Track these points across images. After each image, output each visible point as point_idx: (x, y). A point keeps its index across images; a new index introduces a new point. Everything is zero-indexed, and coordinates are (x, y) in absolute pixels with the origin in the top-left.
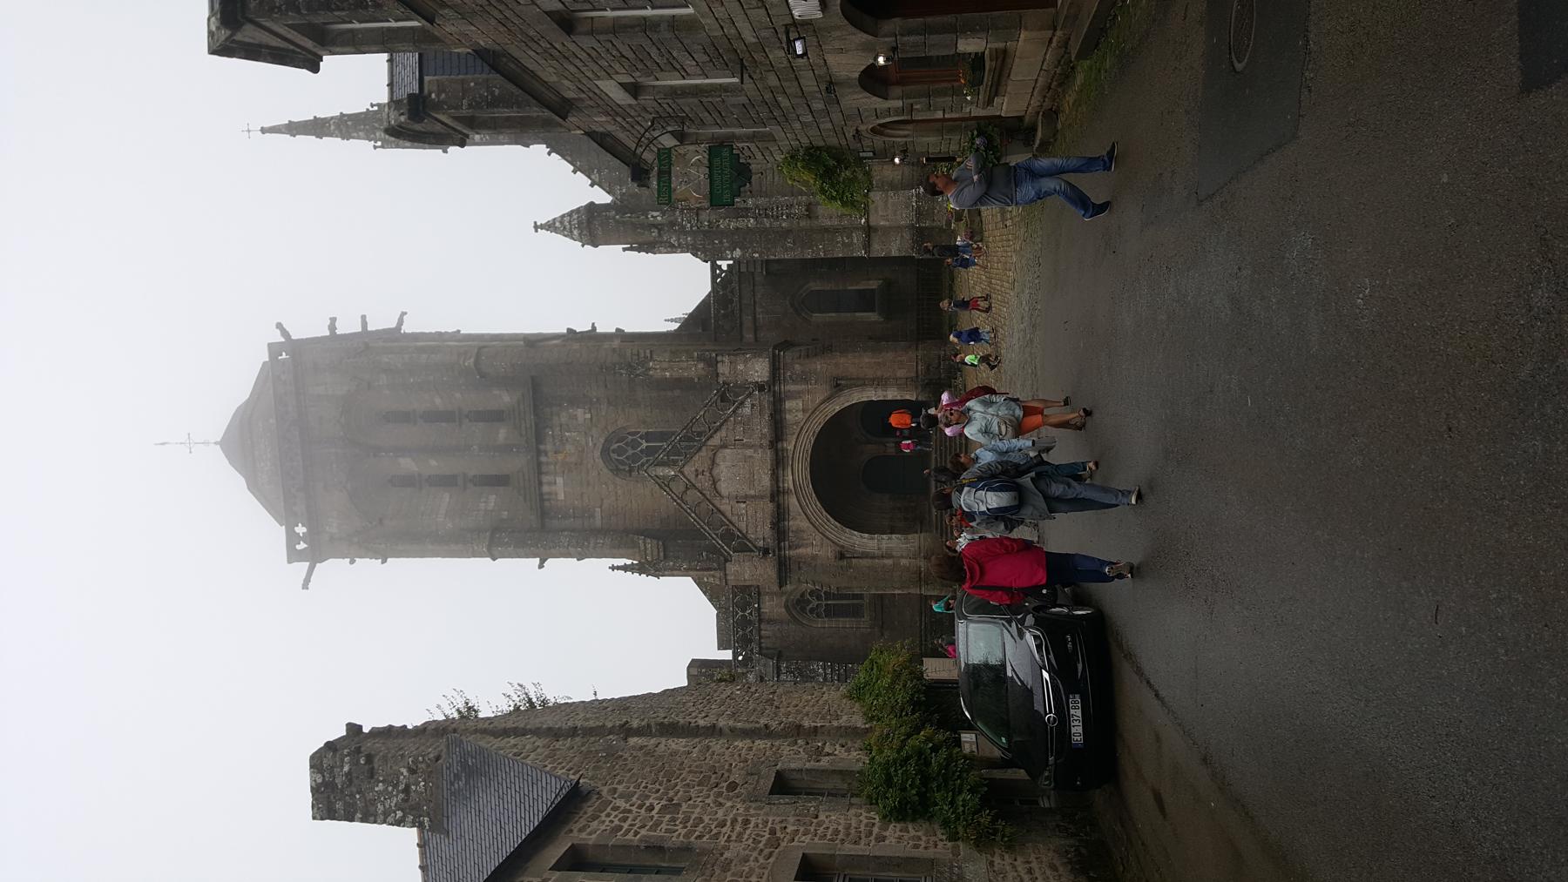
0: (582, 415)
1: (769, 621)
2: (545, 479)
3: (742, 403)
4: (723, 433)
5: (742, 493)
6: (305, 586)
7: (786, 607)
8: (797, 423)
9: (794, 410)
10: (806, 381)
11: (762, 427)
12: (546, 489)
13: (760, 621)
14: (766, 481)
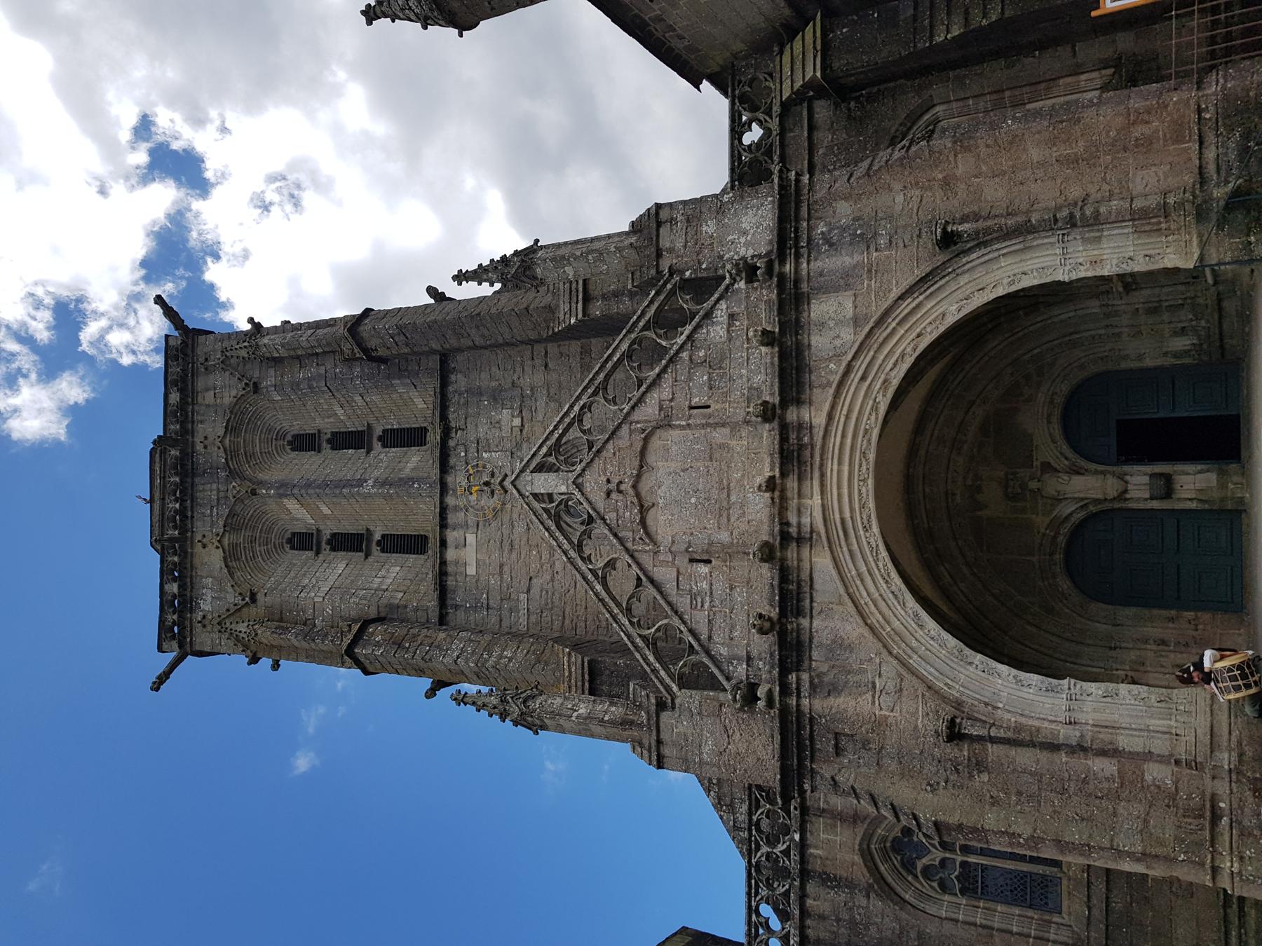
0: (508, 419)
1: (827, 880)
2: (451, 536)
3: (708, 315)
4: (664, 391)
5: (700, 541)
6: (156, 686)
7: (866, 854)
8: (837, 356)
9: (832, 324)
10: (867, 240)
11: (755, 371)
12: (451, 554)
13: (805, 874)
14: (758, 507)
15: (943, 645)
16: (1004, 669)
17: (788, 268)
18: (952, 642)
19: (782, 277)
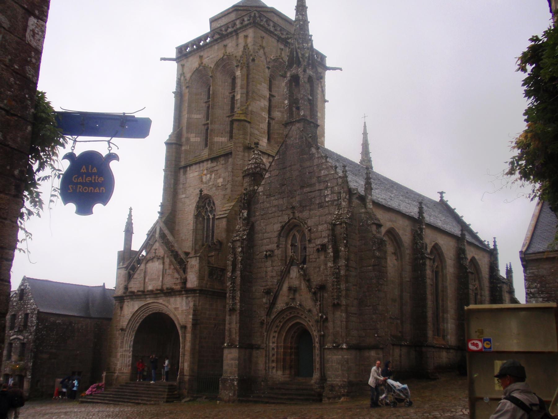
2: (198, 166)
6: (162, 59)
12: (194, 167)
15: (135, 327)
16: (133, 338)
17: (183, 292)
18: (136, 328)
19: (182, 291)
